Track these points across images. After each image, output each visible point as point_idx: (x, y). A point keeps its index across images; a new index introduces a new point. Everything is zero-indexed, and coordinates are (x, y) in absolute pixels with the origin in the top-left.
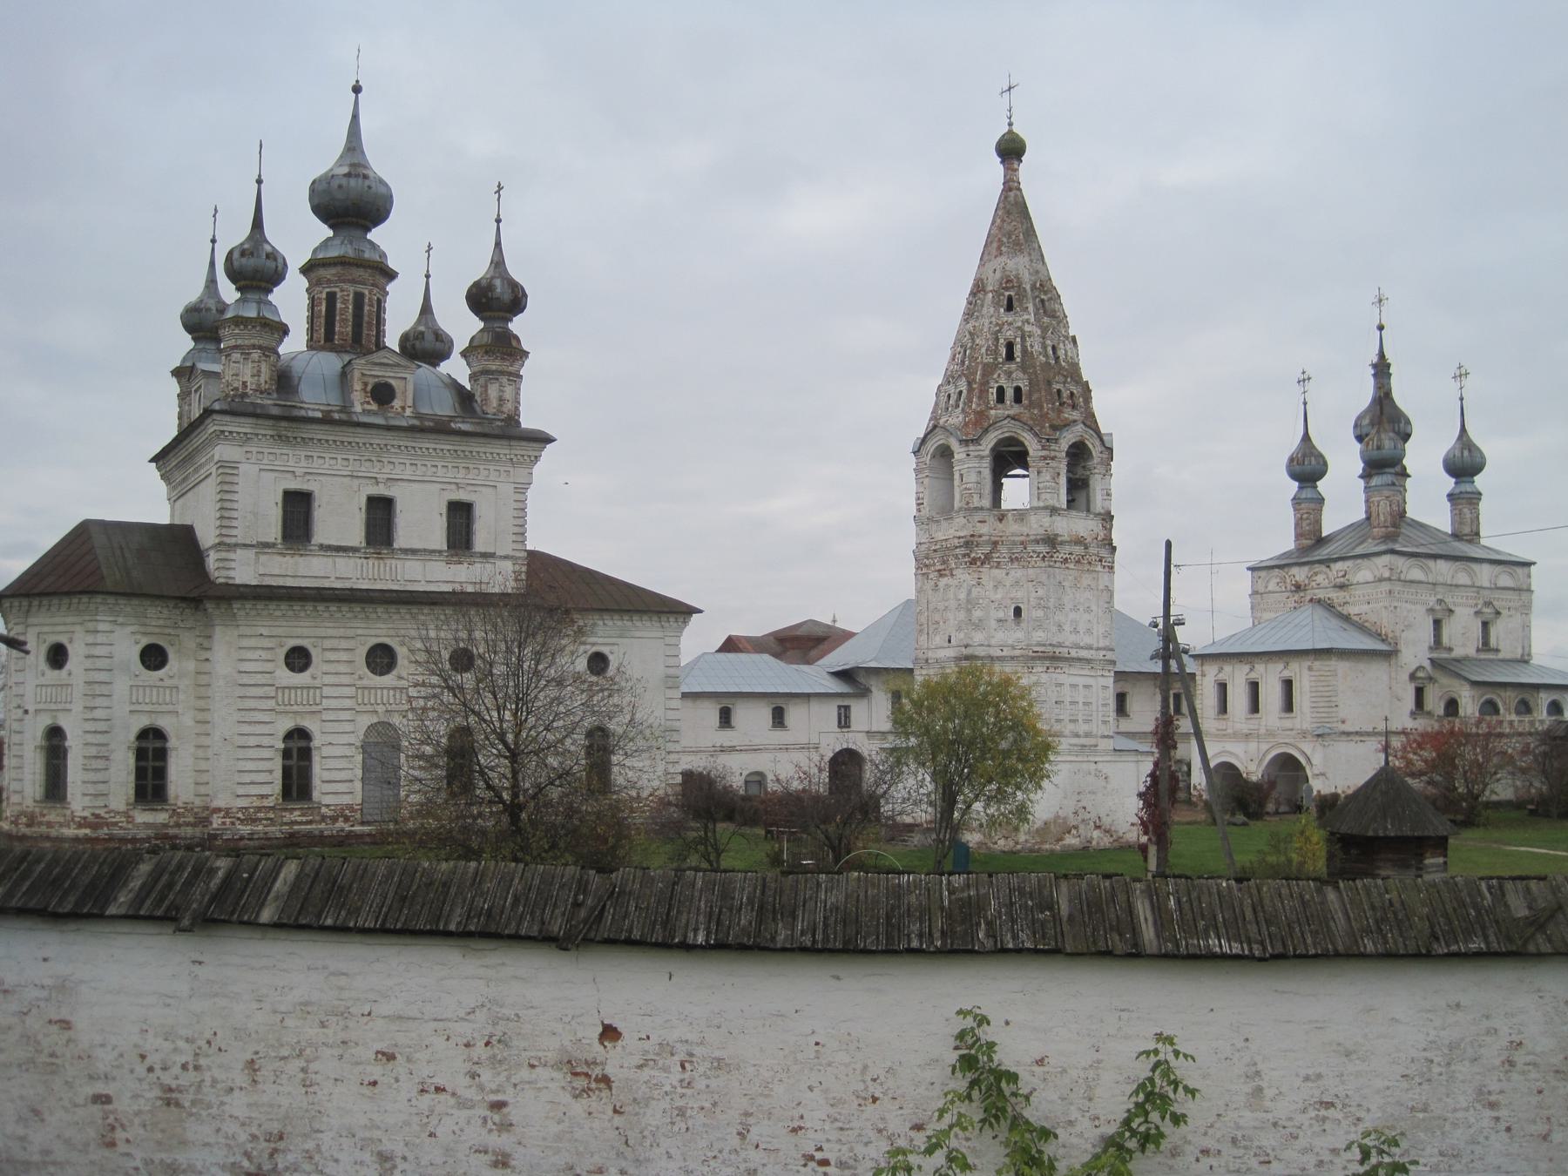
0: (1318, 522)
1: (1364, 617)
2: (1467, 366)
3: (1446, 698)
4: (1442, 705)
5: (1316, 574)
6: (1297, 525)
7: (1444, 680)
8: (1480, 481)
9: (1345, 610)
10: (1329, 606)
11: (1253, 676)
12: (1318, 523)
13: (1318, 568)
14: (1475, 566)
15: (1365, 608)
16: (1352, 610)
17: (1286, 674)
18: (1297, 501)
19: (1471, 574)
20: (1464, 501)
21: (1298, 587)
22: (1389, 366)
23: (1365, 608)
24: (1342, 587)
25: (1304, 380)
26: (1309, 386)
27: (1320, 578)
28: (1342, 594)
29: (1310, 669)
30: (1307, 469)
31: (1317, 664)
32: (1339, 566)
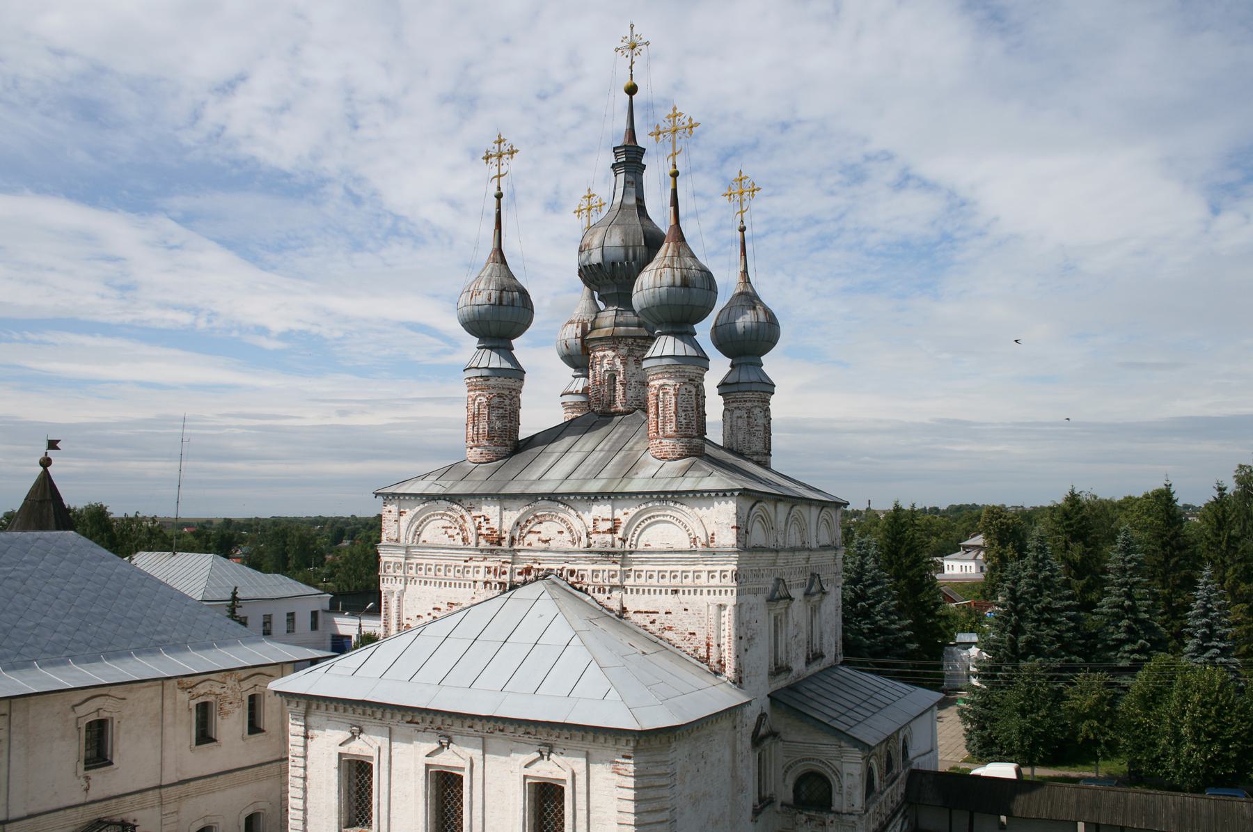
1: (661, 618)
3: (801, 769)
4: (790, 782)
7: (796, 734)
8: (771, 364)
10: (576, 587)
12: (512, 416)
13: (543, 507)
15: (668, 601)
20: (748, 392)
22: (642, 151)
24: (607, 554)
25: (500, 152)
26: (509, 165)
27: (548, 529)
32: (602, 510)
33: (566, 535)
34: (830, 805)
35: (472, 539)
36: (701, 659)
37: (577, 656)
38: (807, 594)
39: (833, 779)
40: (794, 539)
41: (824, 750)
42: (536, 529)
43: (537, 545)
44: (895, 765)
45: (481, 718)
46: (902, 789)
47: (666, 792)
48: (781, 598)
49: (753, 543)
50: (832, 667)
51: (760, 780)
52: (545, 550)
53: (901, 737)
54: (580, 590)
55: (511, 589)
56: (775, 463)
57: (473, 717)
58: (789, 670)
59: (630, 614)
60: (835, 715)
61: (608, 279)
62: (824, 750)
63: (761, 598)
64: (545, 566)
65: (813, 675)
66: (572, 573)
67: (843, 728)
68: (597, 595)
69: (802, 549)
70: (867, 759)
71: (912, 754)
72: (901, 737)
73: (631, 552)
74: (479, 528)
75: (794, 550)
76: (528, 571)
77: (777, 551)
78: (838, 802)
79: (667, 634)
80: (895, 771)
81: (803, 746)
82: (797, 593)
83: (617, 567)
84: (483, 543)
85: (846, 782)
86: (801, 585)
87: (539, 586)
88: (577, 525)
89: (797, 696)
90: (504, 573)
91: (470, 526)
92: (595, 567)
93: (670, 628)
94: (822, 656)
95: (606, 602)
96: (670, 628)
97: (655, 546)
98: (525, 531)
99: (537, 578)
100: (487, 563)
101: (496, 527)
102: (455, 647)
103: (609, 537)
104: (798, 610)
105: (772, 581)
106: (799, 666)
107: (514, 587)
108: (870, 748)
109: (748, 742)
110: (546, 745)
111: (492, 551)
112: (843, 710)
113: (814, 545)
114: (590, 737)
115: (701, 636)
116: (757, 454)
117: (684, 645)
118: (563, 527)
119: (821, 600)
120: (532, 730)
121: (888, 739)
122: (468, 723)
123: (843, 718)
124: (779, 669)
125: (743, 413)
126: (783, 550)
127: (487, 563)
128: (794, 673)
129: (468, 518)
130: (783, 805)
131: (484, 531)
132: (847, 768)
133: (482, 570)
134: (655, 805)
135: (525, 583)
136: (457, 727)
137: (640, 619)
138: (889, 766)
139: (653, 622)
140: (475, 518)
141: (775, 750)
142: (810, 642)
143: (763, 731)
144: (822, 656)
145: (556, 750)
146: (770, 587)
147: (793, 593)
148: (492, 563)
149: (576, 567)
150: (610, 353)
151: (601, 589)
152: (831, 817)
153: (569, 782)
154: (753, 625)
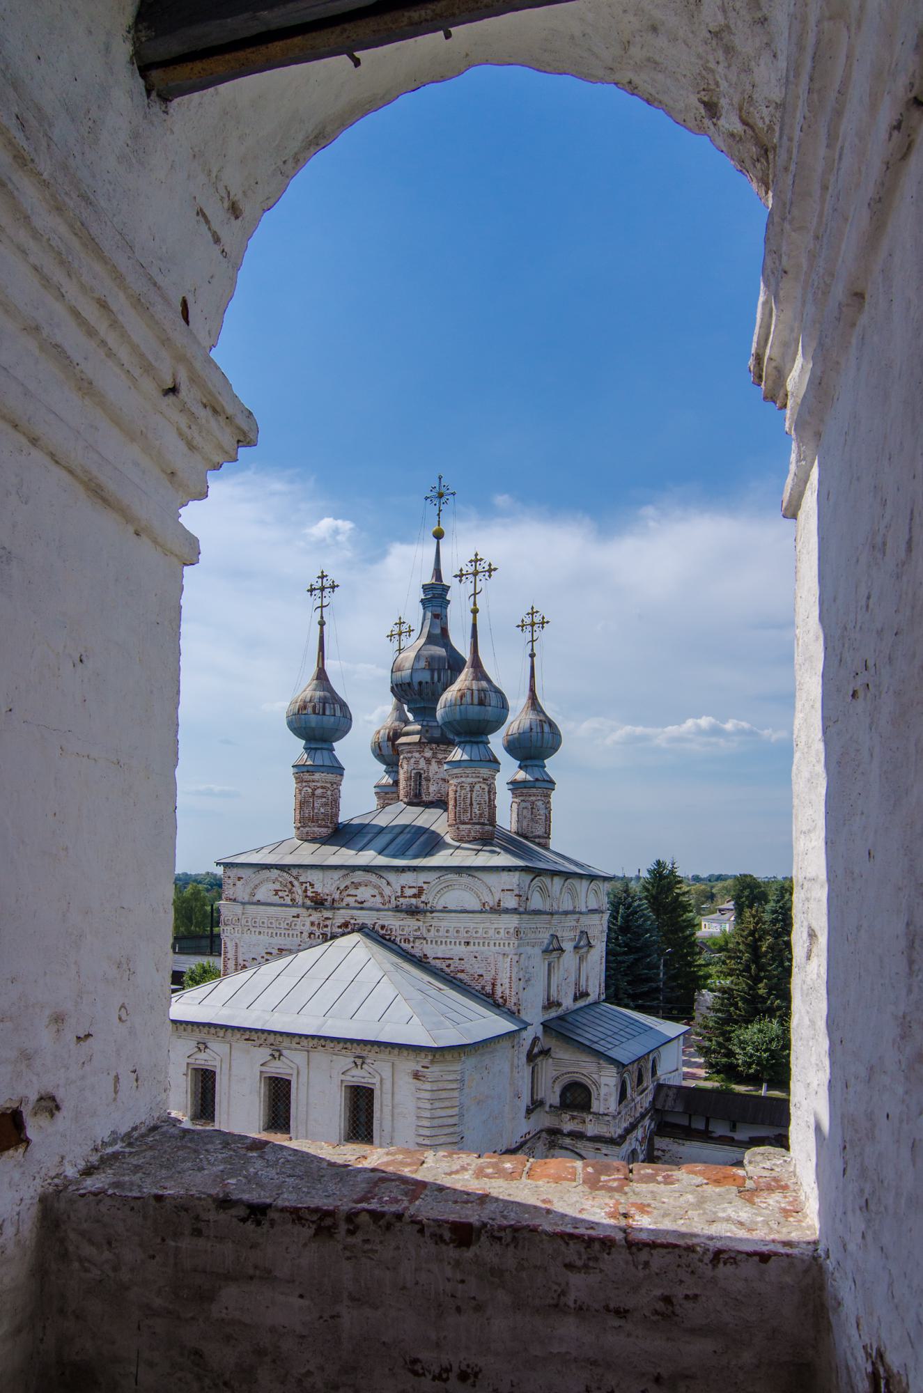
0: (335, 803)
1: (455, 964)
2: (544, 611)
5: (356, 886)
6: (302, 804)
9: (418, 949)
10: (382, 938)
11: (278, 1068)
13: (359, 876)
14: (547, 880)
15: (461, 950)
16: (431, 950)
17: (359, 1076)
18: (302, 771)
19: (574, 895)
21: (318, 903)
23: (461, 950)
24: (413, 912)
27: (364, 893)
28: (411, 924)
29: (416, 1076)
30: (320, 722)
31: (435, 1071)
33: (378, 899)
34: (590, 1107)
35: (299, 900)
36: (488, 995)
37: (387, 990)
38: (576, 947)
39: (593, 1089)
40: (567, 906)
41: (585, 1068)
42: (352, 892)
43: (353, 904)
44: (645, 1079)
45: (307, 1036)
46: (650, 1098)
47: (456, 1094)
48: (555, 950)
49: (532, 908)
50: (596, 1003)
51: (532, 1088)
52: (362, 909)
53: (651, 1058)
54: (389, 940)
55: (332, 938)
56: (554, 844)
57: (300, 1036)
58: (559, 1004)
59: (430, 960)
60: (595, 1039)
61: (414, 693)
62: (585, 1068)
63: (537, 951)
64: (360, 921)
65: (581, 1009)
66: (383, 927)
67: (601, 1049)
68: (403, 945)
69: (573, 912)
70: (621, 1074)
71: (659, 1073)
72: (651, 1058)
73: (432, 912)
74: (305, 891)
75: (566, 913)
76: (346, 925)
77: (552, 914)
78: (596, 1106)
79: (460, 975)
80: (645, 1084)
81: (568, 1063)
82: (568, 946)
83: (420, 923)
84: (308, 903)
85: (603, 1090)
86: (571, 940)
87: (356, 937)
88: (387, 891)
89: (567, 1025)
90: (326, 926)
91: (298, 890)
92: (401, 923)
93: (462, 971)
94: (587, 995)
95: (411, 951)
96: (462, 971)
97: (451, 907)
98: (345, 893)
99: (353, 931)
100: (312, 919)
101: (320, 891)
102: (287, 982)
103: (413, 901)
104: (569, 959)
105: (547, 935)
106: (568, 1003)
107: (334, 937)
108: (624, 1066)
109: (524, 1059)
110: (359, 1057)
111: (316, 909)
112: (603, 1036)
113: (584, 909)
114: (396, 1051)
115: (488, 977)
116: (539, 837)
117: (473, 984)
118: (375, 892)
119: (588, 952)
120: (349, 1045)
121: (639, 1059)
122: (297, 1039)
123: (602, 1042)
124: (550, 1004)
125: (528, 805)
126: (557, 913)
127: (312, 919)
128: (564, 1007)
129: (296, 883)
130: (551, 1106)
131: (309, 893)
132: (604, 1080)
133: (308, 924)
134: (447, 1104)
135: (343, 935)
136: (286, 1042)
137: (438, 963)
138: (640, 1081)
139: (449, 966)
140: (302, 883)
141: (548, 1069)
142: (577, 984)
143: (536, 1050)
144: (587, 995)
145: (368, 1061)
146: (546, 941)
147: (565, 945)
148: (316, 916)
149: (386, 923)
150: (417, 755)
151: (407, 940)
152: (590, 1117)
153: (378, 1086)
154: (531, 970)
